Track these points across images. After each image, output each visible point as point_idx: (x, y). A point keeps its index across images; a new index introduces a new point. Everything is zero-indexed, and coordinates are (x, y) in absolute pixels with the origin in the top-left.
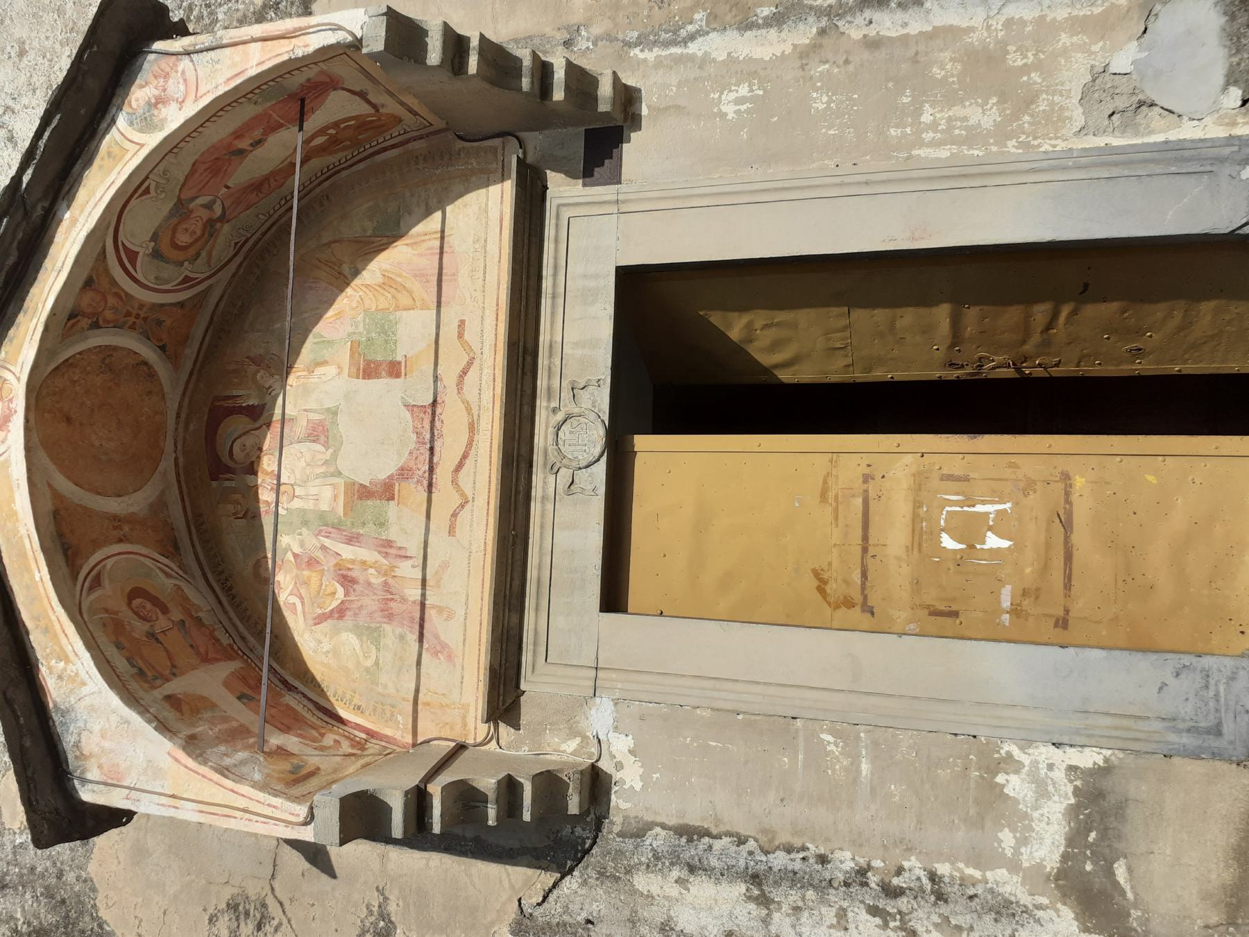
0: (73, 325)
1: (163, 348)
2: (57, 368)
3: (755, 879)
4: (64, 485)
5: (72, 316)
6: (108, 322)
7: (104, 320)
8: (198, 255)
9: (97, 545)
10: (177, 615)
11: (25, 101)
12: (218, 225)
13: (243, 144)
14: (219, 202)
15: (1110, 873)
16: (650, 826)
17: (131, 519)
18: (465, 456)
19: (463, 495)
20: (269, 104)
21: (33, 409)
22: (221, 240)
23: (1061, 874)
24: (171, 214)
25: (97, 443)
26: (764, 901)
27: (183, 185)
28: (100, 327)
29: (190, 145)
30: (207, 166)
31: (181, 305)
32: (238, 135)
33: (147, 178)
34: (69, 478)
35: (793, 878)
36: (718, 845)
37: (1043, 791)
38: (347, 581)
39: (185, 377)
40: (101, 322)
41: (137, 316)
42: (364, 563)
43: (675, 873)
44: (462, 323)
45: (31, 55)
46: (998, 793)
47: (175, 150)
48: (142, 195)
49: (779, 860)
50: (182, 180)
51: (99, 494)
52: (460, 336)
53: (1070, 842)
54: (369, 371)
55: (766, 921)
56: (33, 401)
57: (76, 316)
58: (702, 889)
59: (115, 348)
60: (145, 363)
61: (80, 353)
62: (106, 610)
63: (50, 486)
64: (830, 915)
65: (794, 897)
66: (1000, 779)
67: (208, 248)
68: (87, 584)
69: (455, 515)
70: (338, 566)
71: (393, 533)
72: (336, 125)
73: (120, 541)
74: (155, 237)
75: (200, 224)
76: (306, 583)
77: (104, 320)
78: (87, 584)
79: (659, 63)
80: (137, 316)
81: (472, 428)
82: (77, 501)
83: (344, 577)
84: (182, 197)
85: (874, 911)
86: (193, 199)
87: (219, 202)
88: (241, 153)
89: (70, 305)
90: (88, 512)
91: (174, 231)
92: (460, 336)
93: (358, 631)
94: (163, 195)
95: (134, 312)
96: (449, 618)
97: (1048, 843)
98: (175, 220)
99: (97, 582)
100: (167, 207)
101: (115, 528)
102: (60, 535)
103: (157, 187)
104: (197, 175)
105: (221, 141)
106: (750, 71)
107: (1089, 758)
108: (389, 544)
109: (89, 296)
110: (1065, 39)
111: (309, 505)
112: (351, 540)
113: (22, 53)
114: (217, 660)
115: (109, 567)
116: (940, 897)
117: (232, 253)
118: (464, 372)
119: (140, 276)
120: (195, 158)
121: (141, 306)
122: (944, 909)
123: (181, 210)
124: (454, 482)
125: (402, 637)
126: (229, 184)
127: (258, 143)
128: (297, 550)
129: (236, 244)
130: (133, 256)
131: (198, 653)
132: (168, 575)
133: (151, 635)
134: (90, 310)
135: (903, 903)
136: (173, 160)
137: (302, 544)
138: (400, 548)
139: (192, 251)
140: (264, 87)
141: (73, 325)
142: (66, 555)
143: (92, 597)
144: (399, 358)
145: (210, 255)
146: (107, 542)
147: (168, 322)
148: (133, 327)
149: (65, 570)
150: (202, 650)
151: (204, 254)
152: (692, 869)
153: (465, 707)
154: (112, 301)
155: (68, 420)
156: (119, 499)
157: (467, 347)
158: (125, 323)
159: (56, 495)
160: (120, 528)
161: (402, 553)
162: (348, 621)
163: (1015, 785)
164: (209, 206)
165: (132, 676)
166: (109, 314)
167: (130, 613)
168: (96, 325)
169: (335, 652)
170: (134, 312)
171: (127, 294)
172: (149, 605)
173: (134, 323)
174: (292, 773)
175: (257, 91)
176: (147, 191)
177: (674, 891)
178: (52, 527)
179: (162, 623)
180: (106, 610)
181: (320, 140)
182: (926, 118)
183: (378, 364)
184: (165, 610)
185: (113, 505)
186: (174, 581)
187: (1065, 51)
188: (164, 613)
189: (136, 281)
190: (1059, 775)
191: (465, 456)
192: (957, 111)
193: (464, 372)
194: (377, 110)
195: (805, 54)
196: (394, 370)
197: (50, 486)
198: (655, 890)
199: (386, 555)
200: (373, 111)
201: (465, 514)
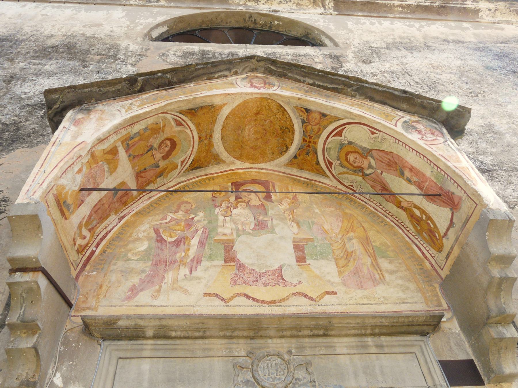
0: (302, 111)
1: (295, 157)
2: (282, 106)
4: (225, 112)
5: (308, 111)
6: (306, 128)
7: (306, 126)
8: (344, 167)
9: (198, 126)
10: (162, 164)
12: (361, 174)
13: (407, 173)
14: (373, 171)
17: (210, 145)
18: (254, 299)
19: (231, 299)
20: (433, 178)
21: (261, 96)
22: (354, 177)
24: (363, 148)
25: (247, 128)
27: (379, 150)
28: (303, 124)
29: (401, 147)
30: (391, 159)
31: (318, 163)
32: (412, 169)
33: (380, 131)
34: (230, 114)
38: (178, 243)
39: (283, 170)
40: (305, 124)
41: (310, 142)
42: (188, 250)
44: (336, 293)
47: (397, 141)
48: (371, 131)
50: (382, 149)
51: (223, 128)
52: (327, 293)
54: (298, 247)
56: (265, 96)
57: (307, 112)
59: (293, 134)
60: (287, 149)
61: (289, 116)
62: (164, 126)
63: (225, 104)
67: (348, 171)
68: (178, 118)
69: (217, 296)
70: (186, 238)
71: (205, 263)
72: (429, 218)
73: (200, 138)
74: (350, 143)
75: (360, 164)
76: (178, 224)
77: (306, 126)
78: (178, 118)
80: (310, 142)
81: (272, 303)
82: (219, 117)
83: (180, 241)
84: (373, 152)
86: (373, 157)
87: (373, 171)
88: (402, 174)
89: (312, 108)
90: (213, 122)
91: (354, 152)
92: (327, 293)
93: (149, 248)
94: (372, 142)
95: (312, 140)
96: (153, 297)
98: (360, 151)
99: (179, 124)
100: (366, 145)
101: (206, 136)
102: (202, 108)
103: (375, 137)
104: (386, 156)
105: (406, 162)
108: (199, 262)
109: (317, 116)
111: (220, 223)
112: (202, 244)
114: (137, 182)
115: (187, 131)
117: (347, 184)
118: (306, 296)
119: (330, 139)
120: (395, 152)
121: (315, 143)
123: (366, 153)
124: (238, 294)
125: (143, 271)
126: (384, 174)
127: (409, 181)
128: (196, 219)
129: (352, 186)
130: (339, 134)
131: (141, 172)
132: (182, 162)
133: (151, 148)
134: (311, 118)
136: (392, 141)
137: (199, 221)
138: (196, 268)
139: (345, 163)
140: (443, 173)
141: (302, 111)
142: (192, 109)
143: (171, 120)
144: (308, 262)
145: (345, 173)
146: (199, 131)
147: (308, 158)
148: (304, 140)
149: (185, 108)
150: (143, 174)
151: (345, 170)
153: (96, 309)
154: (316, 128)
155: (257, 114)
156: (220, 139)
157: (321, 296)
158: (306, 136)
159: (221, 107)
160: (206, 139)
161: (194, 268)
162: (154, 244)
164: (370, 166)
165: (129, 133)
166: (309, 127)
167: (163, 139)
168: (303, 122)
169: (137, 239)
170: (312, 140)
171: (320, 135)
172: (167, 149)
173: (306, 141)
174: (65, 202)
175: (439, 170)
176: (373, 133)
178: (205, 104)
179: (158, 156)
180: (164, 126)
181: (417, 213)
183: (303, 251)
184: (165, 158)
185: (217, 136)
186: (180, 164)
188: (163, 157)
189: (325, 143)
191: (254, 299)
193: (306, 296)
194: (443, 237)
196: (301, 259)
197: (225, 104)
199: (192, 260)
200: (442, 234)
201: (217, 302)
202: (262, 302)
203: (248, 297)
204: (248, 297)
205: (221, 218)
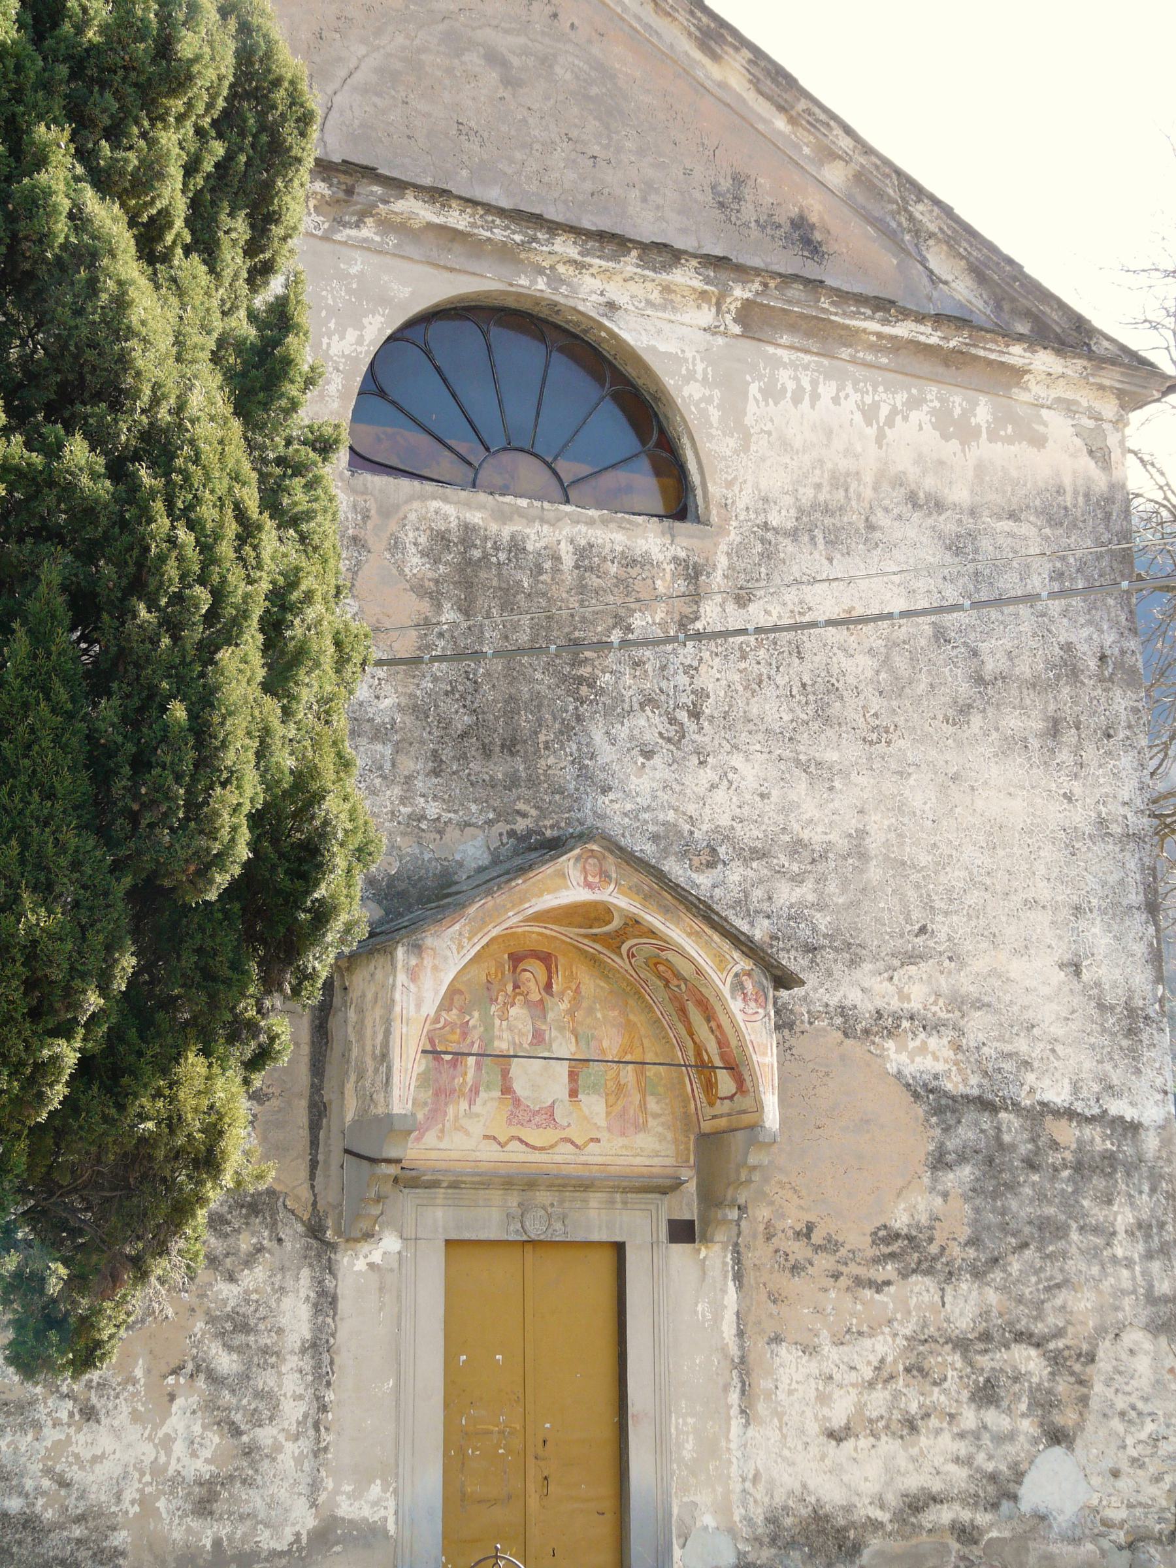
3: (314, 1345)
11: (734, 799)
15: (337, 1543)
16: (335, 1277)
18: (527, 1144)
19: (506, 1143)
23: (334, 1518)
26: (303, 1351)
35: (318, 1366)
36: (329, 1320)
37: (375, 1504)
43: (312, 1295)
44: (598, 1141)
45: (760, 805)
46: (371, 1481)
49: (326, 1357)
52: (592, 1140)
53: (351, 1521)
55: (292, 1352)
58: (305, 1311)
64: (300, 1390)
65: (308, 1368)
66: (378, 1482)
69: (495, 1138)
76: (452, 1031)
79: (725, 1264)
81: (542, 1149)
85: (306, 1416)
88: (708, 1021)
92: (592, 1140)
97: (346, 1509)
106: (717, 1318)
107: (391, 1527)
108: (477, 1093)
110: (720, 1490)
111: (497, 1033)
113: (762, 796)
116: (316, 1454)
118: (573, 1143)
122: (311, 1455)
124: (513, 1138)
135: (311, 1432)
137: (474, 1027)
152: (315, 1305)
157: (586, 1144)
163: (376, 1489)
177: (302, 1295)
182: (690, 1420)
183: (576, 1081)
187: (714, 1490)
190: (382, 1513)
191: (527, 1144)
192: (691, 1437)
193: (573, 1143)
195: (724, 1349)
196: (573, 1093)
198: (302, 1282)
201: (497, 1147)
202: (534, 1148)
203: (521, 1141)
204: (521, 1141)
205: (497, 1022)
